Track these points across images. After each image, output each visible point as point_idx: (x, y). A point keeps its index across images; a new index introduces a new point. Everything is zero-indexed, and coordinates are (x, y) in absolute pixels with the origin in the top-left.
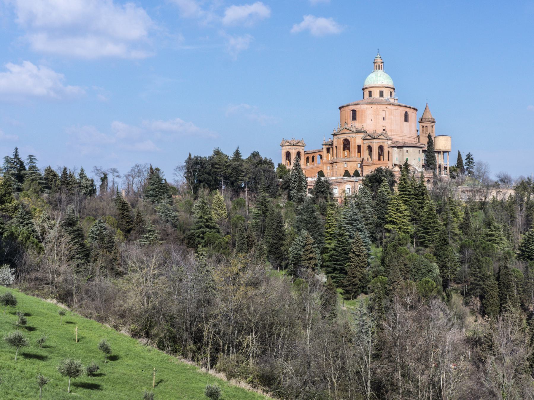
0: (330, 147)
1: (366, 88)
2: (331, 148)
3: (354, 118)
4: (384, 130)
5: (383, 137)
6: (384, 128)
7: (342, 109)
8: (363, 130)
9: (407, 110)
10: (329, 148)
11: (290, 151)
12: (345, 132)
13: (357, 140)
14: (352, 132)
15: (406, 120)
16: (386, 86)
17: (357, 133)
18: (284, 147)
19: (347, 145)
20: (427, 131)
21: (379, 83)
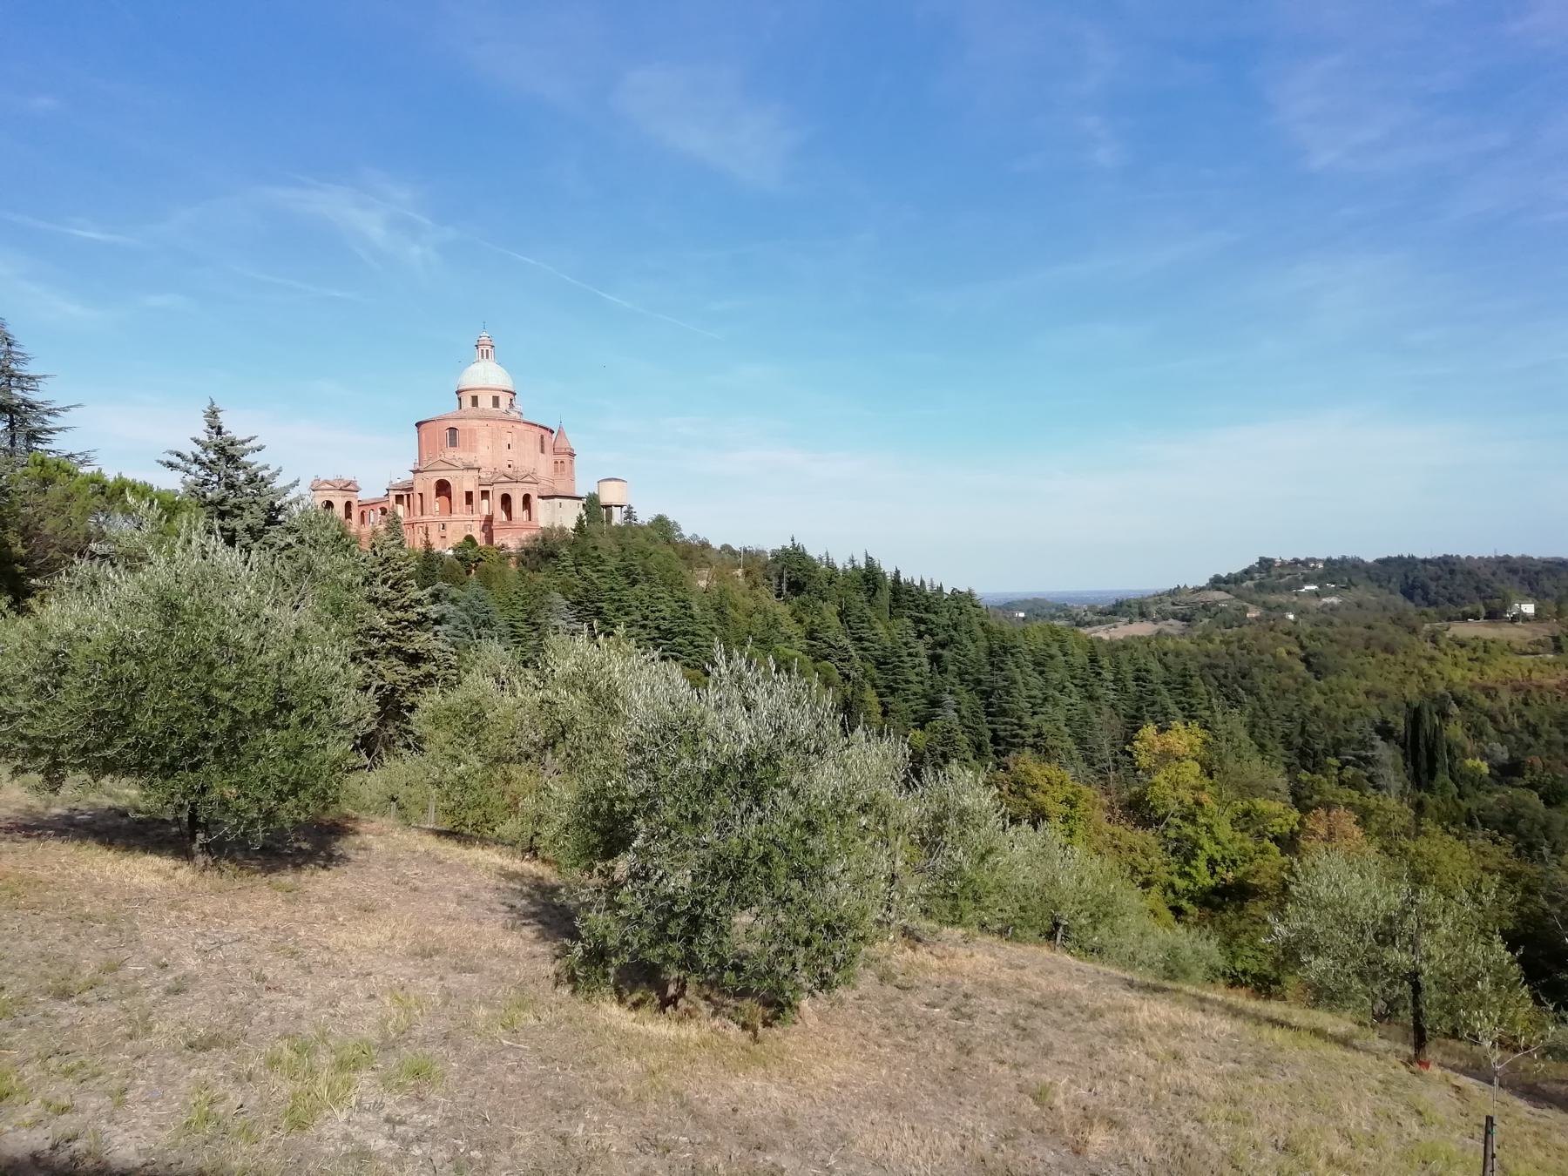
0: (403, 493)
1: (467, 390)
2: (405, 497)
3: (453, 443)
4: (510, 466)
5: (530, 480)
6: (510, 463)
7: (423, 426)
8: (475, 466)
9: (543, 432)
10: (402, 496)
11: (331, 499)
12: (439, 468)
13: (462, 483)
14: (455, 468)
15: (542, 451)
16: (505, 388)
17: (465, 472)
18: (319, 492)
19: (443, 488)
20: (563, 469)
21: (492, 383)
